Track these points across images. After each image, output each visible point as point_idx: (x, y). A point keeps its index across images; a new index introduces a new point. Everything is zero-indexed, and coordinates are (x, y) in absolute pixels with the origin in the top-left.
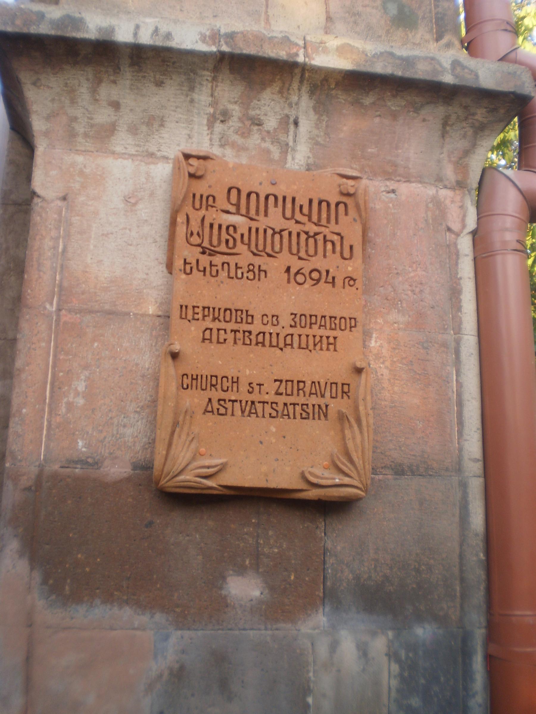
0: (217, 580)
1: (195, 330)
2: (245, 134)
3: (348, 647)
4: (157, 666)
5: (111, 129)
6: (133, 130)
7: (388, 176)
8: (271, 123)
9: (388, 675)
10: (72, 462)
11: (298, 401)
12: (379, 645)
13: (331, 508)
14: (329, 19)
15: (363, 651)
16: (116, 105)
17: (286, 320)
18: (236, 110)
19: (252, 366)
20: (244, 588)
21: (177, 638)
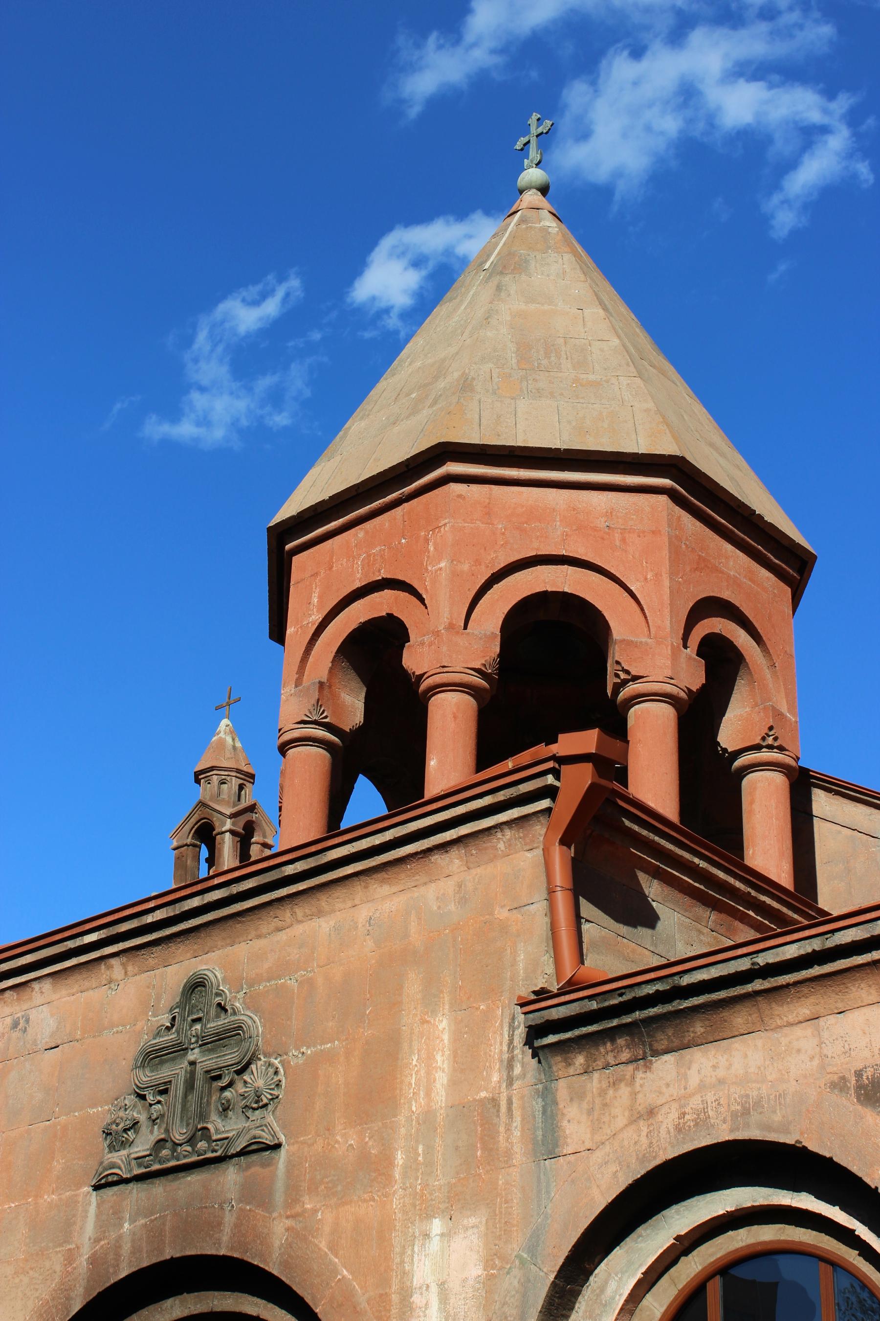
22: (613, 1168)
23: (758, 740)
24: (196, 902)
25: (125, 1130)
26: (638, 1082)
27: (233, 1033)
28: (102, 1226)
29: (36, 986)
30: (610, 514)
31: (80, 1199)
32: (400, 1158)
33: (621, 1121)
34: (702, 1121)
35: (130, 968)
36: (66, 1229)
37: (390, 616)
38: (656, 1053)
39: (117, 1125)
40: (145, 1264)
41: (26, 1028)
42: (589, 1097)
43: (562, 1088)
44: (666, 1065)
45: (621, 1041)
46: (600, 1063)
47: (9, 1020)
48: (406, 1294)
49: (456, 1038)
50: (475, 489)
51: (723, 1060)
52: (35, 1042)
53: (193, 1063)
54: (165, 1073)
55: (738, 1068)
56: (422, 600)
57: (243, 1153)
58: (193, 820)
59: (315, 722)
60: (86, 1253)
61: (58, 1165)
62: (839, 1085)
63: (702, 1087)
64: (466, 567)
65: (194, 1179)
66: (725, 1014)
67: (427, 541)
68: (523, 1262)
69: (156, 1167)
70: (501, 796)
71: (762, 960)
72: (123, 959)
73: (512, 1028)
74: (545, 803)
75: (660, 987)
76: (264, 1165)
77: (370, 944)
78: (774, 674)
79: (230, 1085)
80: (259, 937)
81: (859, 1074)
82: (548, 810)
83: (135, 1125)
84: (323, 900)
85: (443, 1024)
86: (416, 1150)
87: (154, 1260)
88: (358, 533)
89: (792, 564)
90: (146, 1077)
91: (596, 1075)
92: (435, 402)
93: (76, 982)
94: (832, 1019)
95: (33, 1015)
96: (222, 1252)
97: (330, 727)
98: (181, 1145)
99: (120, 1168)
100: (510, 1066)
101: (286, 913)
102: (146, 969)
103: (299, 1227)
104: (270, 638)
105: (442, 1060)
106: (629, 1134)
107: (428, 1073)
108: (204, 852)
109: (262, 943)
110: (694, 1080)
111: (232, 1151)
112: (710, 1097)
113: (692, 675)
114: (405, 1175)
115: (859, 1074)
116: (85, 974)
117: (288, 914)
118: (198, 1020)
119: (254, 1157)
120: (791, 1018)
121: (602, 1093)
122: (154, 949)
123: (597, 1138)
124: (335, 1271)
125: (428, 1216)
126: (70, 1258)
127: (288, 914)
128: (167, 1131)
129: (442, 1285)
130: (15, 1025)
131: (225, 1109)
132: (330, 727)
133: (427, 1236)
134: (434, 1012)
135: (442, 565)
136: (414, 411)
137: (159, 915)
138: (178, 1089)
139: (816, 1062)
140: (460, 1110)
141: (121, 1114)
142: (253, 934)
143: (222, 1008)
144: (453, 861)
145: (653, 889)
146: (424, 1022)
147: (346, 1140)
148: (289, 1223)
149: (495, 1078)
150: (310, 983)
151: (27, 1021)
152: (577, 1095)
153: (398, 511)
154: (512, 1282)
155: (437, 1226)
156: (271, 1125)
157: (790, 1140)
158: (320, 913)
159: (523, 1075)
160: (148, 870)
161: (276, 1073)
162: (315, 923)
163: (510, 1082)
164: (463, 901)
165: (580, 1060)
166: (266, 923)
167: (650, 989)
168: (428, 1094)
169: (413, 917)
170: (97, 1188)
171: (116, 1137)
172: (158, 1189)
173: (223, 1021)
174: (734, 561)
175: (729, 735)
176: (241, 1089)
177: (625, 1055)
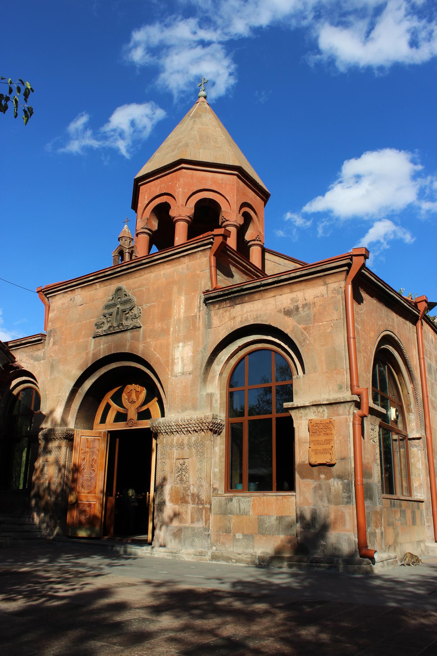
0: (319, 475)
1: (313, 444)
2: (318, 414)
3: (336, 483)
4: (313, 486)
5: (302, 417)
6: (304, 416)
7: (338, 415)
8: (321, 411)
9: (341, 487)
10: (302, 462)
11: (325, 451)
12: (340, 483)
13: (332, 465)
14: (329, 391)
15: (337, 483)
16: (301, 413)
17: (323, 441)
18: (316, 411)
19: (320, 447)
20: (322, 476)
21: (315, 483)
22: (225, 330)
23: (255, 238)
24: (119, 269)
26: (231, 311)
27: (129, 301)
28: (95, 346)
29: (76, 290)
30: (222, 180)
32: (172, 329)
33: (227, 320)
34: (246, 320)
36: (86, 348)
37: (166, 202)
38: (236, 304)
42: (219, 315)
43: (212, 313)
44: (238, 307)
45: (227, 302)
46: (222, 307)
47: (69, 299)
48: (173, 360)
49: (186, 301)
50: (189, 171)
51: (252, 306)
52: (76, 304)
53: (118, 308)
54: (111, 310)
55: (256, 307)
56: (175, 198)
57: (132, 329)
58: (118, 250)
59: (146, 228)
60: (91, 353)
61: (83, 333)
62: (280, 311)
63: (247, 312)
64: (186, 191)
65: (119, 335)
66: (253, 295)
67: (176, 183)
68: (202, 352)
69: (109, 332)
70: (199, 244)
71: (263, 283)
73: (200, 299)
74: (210, 246)
75: (238, 289)
76: (137, 332)
77: (164, 279)
78: (259, 222)
79: (128, 313)
80: (135, 278)
81: (284, 309)
82: (211, 248)
84: (152, 269)
85: (183, 298)
86: (176, 327)
87: (109, 354)
88: (158, 181)
89: (265, 196)
90: (106, 311)
91: (221, 310)
92: (179, 149)
93: (87, 289)
94: (278, 297)
95: (76, 297)
96: (126, 352)
97: (149, 230)
100: (200, 308)
101: (142, 272)
103: (146, 345)
104: (132, 208)
105: (182, 307)
106: (229, 323)
107: (179, 310)
108: (120, 258)
109: (136, 279)
110: (245, 310)
111: (129, 328)
112: (249, 314)
113: (241, 221)
114: (173, 333)
115: (284, 309)
116: (89, 287)
117: (143, 272)
118: (120, 298)
119: (134, 330)
120: (269, 296)
121: (222, 314)
123: (221, 324)
124: (155, 355)
125: (179, 342)
126: (87, 354)
127: (143, 272)
128: (112, 324)
129: (182, 358)
130: (71, 300)
131: (127, 319)
132: (149, 230)
133: (178, 347)
134: (181, 296)
135: (180, 190)
136: (173, 151)
137: (109, 272)
138: (115, 314)
139: (274, 306)
140: (187, 318)
141: (100, 320)
142: (134, 277)
143: (126, 295)
144: (186, 260)
145: (233, 269)
146: (178, 298)
147: (158, 325)
148: (143, 345)
149: (196, 310)
150: (149, 289)
151: (74, 299)
152: (216, 314)
153: (169, 176)
154: (200, 356)
155: (181, 344)
156: (139, 322)
157: (267, 324)
158: (151, 272)
159: (203, 310)
160: (107, 262)
161: (140, 310)
162: (149, 275)
163: (200, 311)
164: (188, 269)
165: (217, 306)
166: (137, 275)
167: (236, 289)
168: (179, 314)
169: (175, 273)
170: (94, 338)
171: (98, 326)
172: (110, 338)
173: (126, 298)
174: (251, 194)
175: (248, 236)
176: (131, 314)
177: (228, 305)
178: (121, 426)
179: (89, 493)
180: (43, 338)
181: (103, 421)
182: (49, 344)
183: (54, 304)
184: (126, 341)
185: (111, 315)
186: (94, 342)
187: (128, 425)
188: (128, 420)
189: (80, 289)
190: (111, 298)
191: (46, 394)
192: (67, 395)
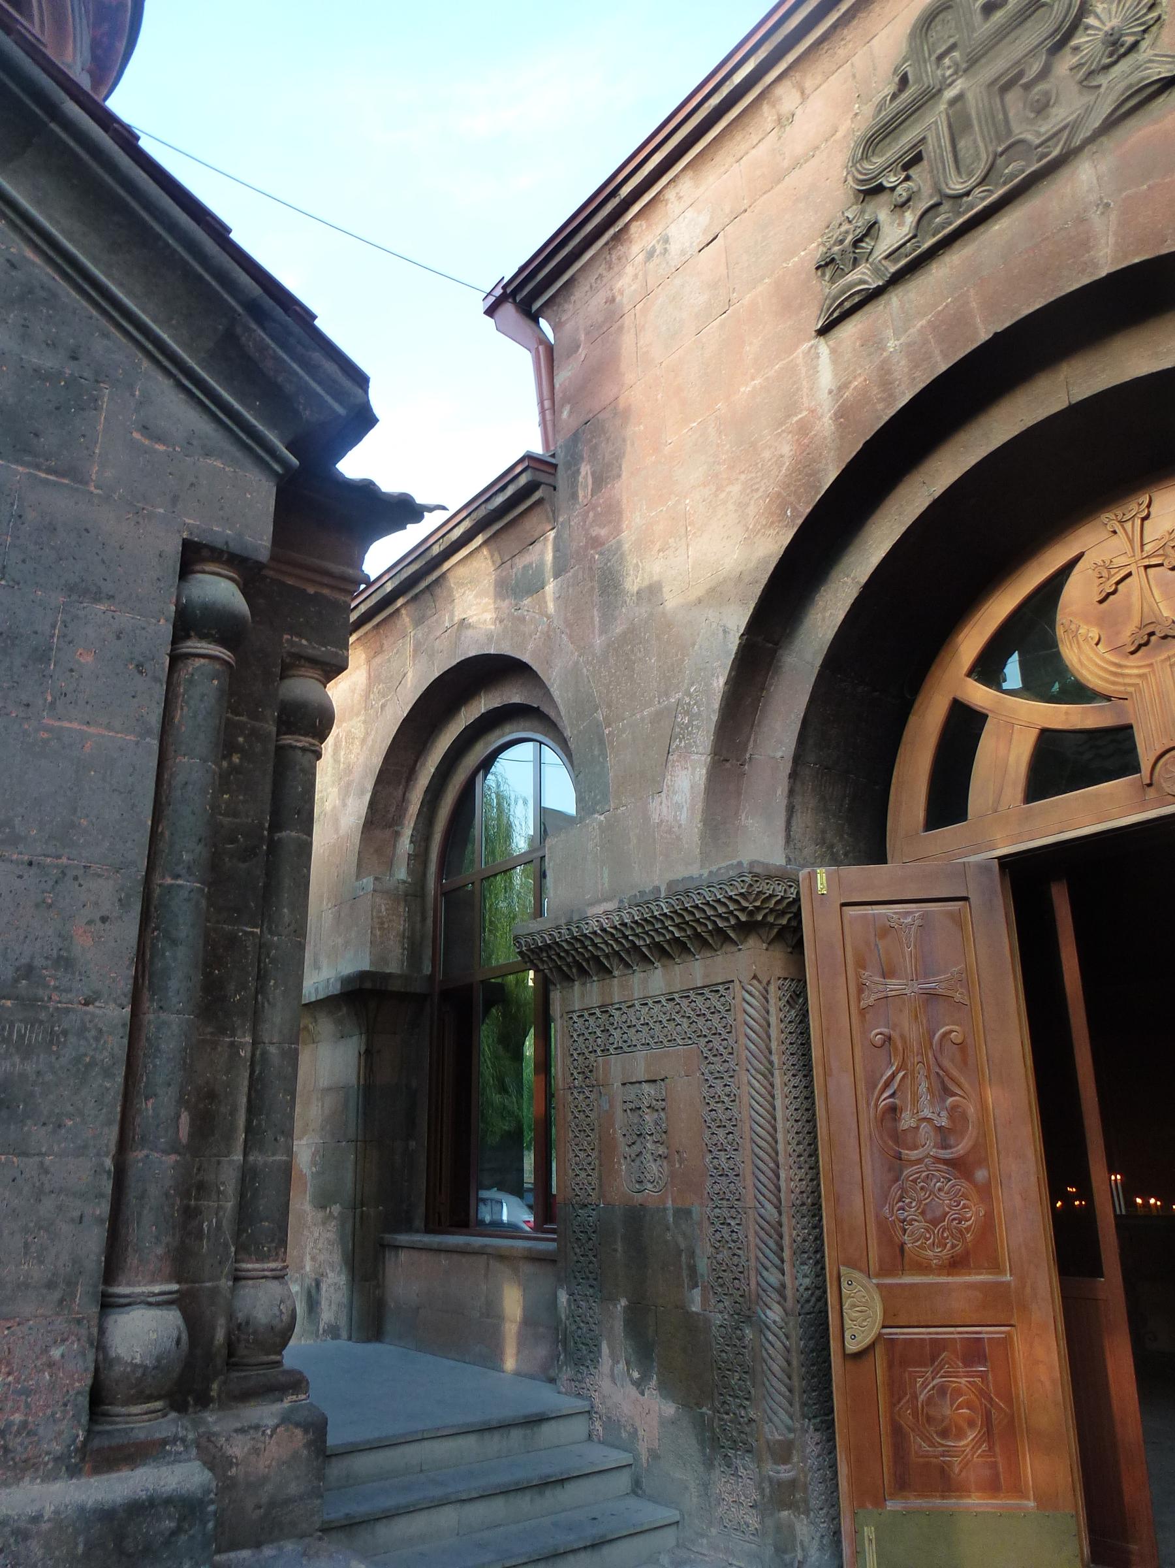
25: (856, 243)
31: (800, 361)
35: (809, 84)
39: (841, 242)
40: (943, 367)
41: (666, 249)
47: (641, 257)
53: (960, 97)
72: (797, 76)
83: (872, 229)
95: (673, 231)
98: (968, 194)
99: (865, 282)
102: (835, 68)
111: (1077, 142)
116: (738, 136)
118: (953, 47)
122: (845, 31)
130: (650, 255)
131: (1042, 108)
170: (823, 332)
172: (940, 271)
178: (1099, 809)
179: (956, 1264)
180: (542, 478)
181: (948, 801)
182: (574, 496)
183: (568, 326)
184: (1081, 220)
185: (917, 159)
186: (833, 351)
187: (1151, 793)
188: (1146, 759)
189: (690, 173)
190: (891, 89)
191: (598, 725)
192: (719, 683)
